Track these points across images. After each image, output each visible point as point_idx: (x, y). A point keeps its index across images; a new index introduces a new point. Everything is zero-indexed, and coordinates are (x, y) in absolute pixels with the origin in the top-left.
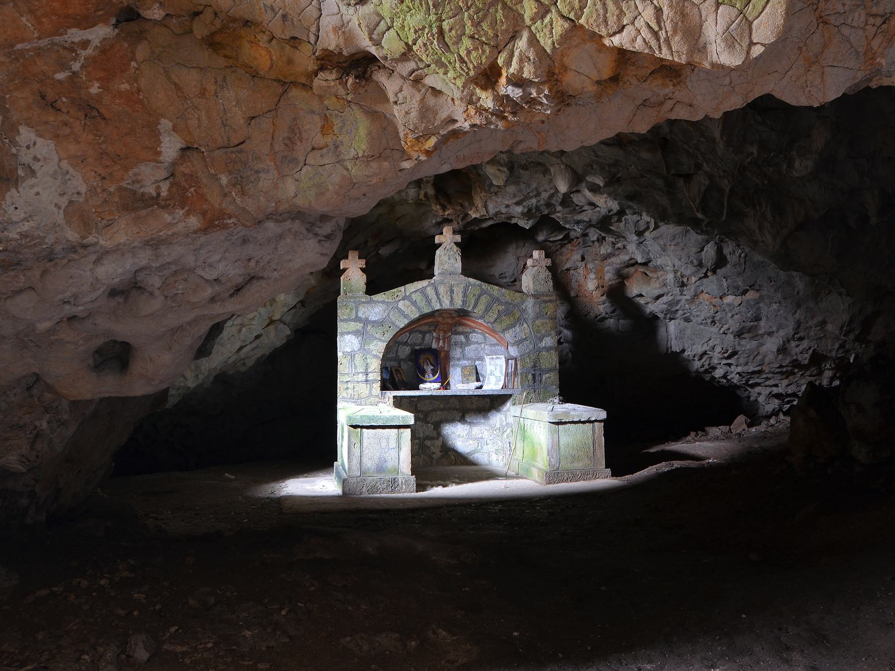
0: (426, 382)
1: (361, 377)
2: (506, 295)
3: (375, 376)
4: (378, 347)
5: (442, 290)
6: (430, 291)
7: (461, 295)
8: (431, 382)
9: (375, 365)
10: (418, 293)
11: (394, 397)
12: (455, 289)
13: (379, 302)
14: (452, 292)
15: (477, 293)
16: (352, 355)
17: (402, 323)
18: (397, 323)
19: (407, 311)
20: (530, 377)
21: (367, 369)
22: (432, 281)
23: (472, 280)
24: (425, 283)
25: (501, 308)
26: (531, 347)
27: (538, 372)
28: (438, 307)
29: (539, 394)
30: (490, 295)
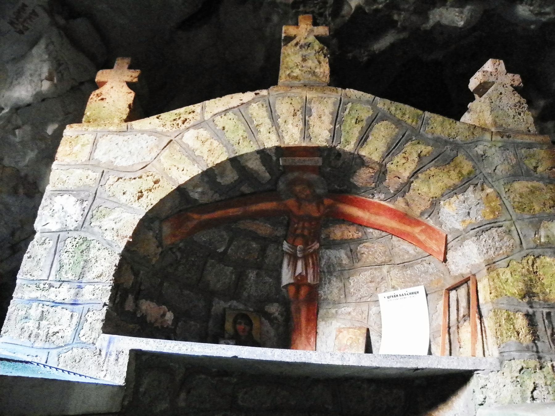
2: (438, 125)
3: (98, 294)
4: (120, 224)
7: (327, 119)
9: (105, 264)
10: (230, 115)
11: (136, 356)
12: (315, 108)
13: (143, 132)
14: (306, 111)
16: (59, 237)
19: (202, 151)
20: (521, 322)
21: (82, 275)
22: (264, 92)
25: (426, 149)
30: (398, 123)
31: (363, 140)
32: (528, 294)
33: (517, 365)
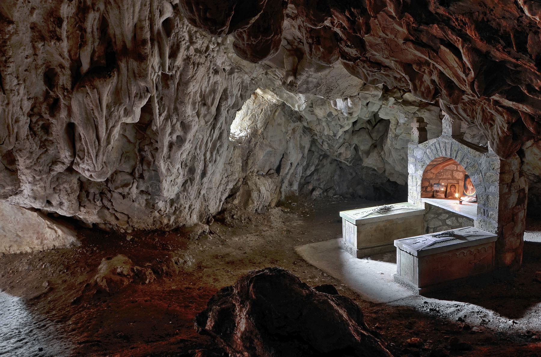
0: (467, 195)
1: (415, 188)
5: (442, 145)
6: (437, 146)
7: (449, 149)
8: (469, 196)
15: (457, 149)
17: (428, 162)
18: (427, 162)
20: (482, 210)
23: (454, 140)
24: (435, 140)
26: (484, 190)
27: (486, 209)
28: (441, 155)
29: (486, 224)
31: (456, 157)
32: (484, 205)
33: (480, 220)
